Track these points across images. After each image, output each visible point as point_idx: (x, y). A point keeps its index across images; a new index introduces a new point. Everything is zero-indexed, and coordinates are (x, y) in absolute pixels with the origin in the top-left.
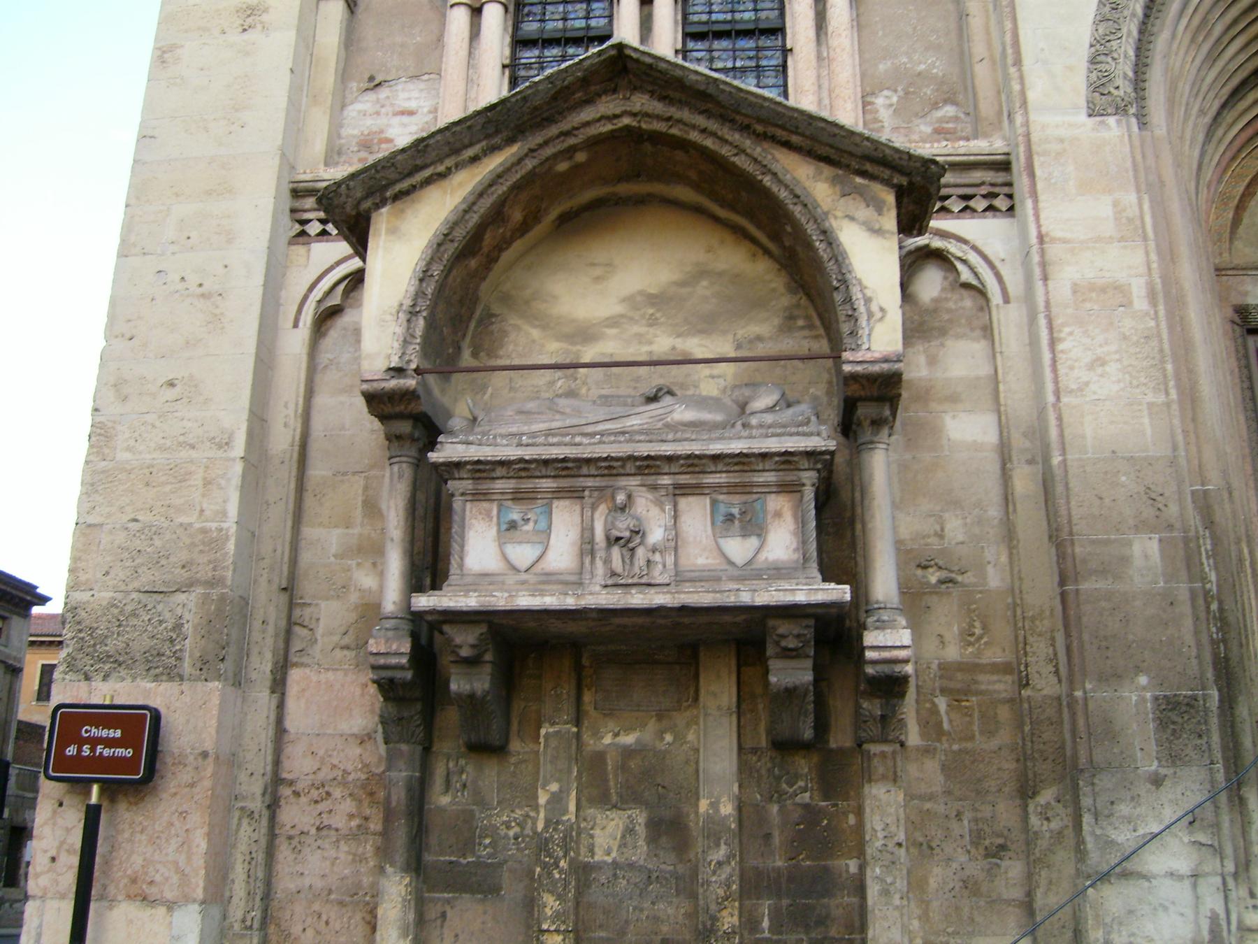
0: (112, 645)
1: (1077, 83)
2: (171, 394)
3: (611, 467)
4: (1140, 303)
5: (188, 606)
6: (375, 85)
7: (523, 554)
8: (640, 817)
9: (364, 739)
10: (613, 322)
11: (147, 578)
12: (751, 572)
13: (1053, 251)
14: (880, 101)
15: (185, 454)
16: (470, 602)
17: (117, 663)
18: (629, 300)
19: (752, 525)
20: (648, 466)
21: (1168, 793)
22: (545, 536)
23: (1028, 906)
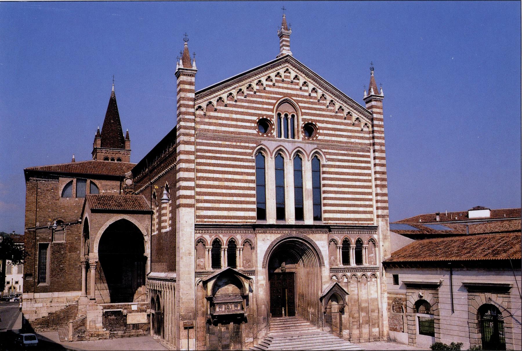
0: (185, 318)
1: (261, 265)
2: (187, 295)
3: (228, 303)
4: (264, 286)
5: (191, 314)
6: (199, 258)
7: (221, 310)
8: (225, 327)
9: (203, 323)
10: (222, 285)
11: (188, 312)
12: (237, 310)
13: (258, 281)
14: (244, 262)
15: (189, 300)
16: (218, 314)
17: (185, 319)
18: (223, 283)
19: (237, 307)
20: (230, 303)
21: (264, 324)
22: (222, 308)
23: (253, 333)
